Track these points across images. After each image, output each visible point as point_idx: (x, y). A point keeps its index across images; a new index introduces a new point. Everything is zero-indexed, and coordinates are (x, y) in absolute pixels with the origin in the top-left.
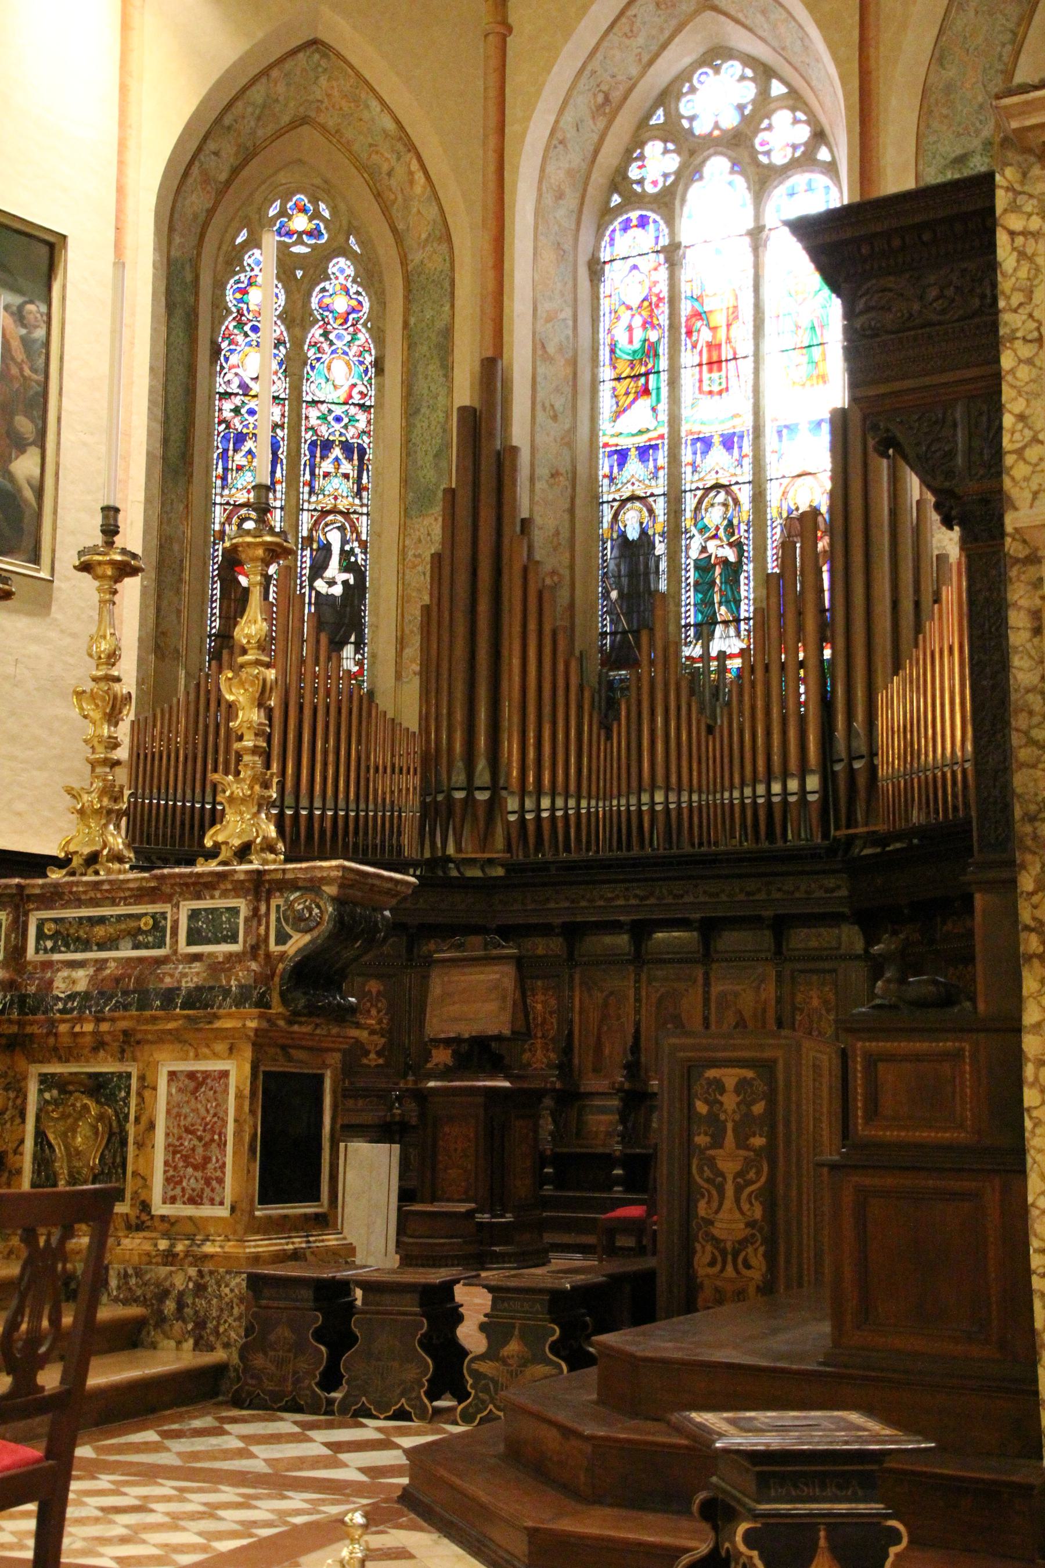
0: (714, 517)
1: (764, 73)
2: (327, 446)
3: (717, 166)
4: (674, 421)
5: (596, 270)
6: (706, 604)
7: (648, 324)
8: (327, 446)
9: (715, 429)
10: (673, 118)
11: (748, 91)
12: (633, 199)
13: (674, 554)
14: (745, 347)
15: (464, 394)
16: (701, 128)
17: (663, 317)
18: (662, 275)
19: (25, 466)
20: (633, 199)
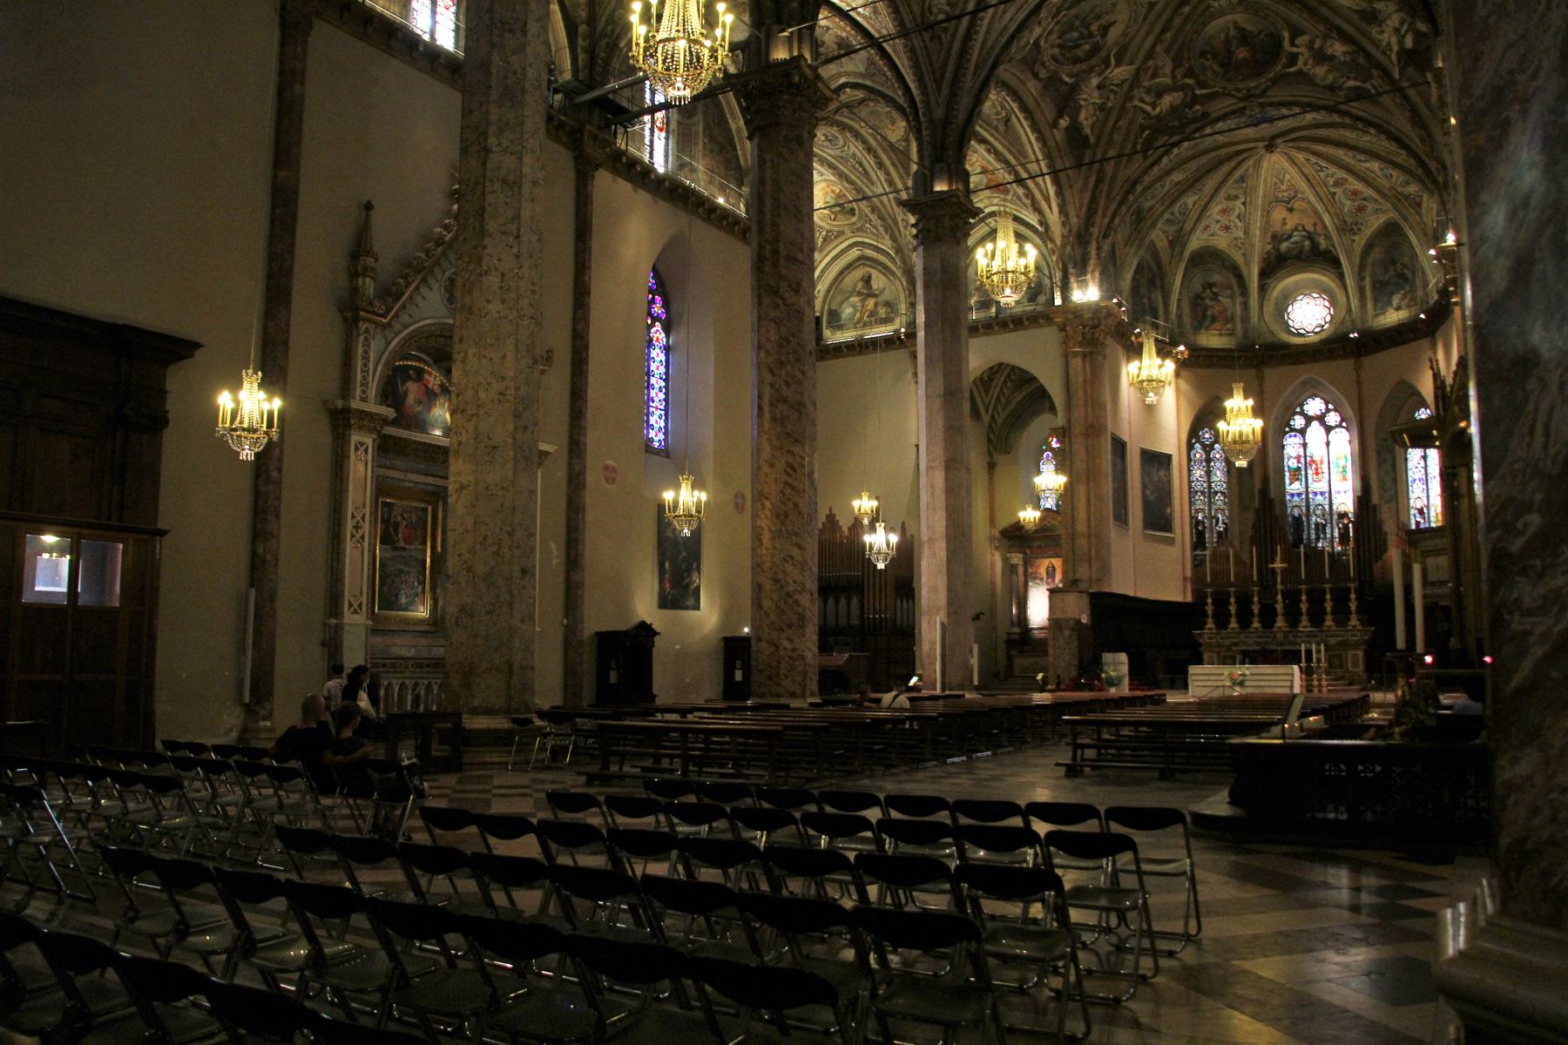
0: (1318, 512)
1: (1327, 403)
2: (1216, 493)
3: (1315, 424)
4: (1307, 487)
5: (1283, 447)
6: (1317, 534)
7: (1299, 462)
8: (1216, 493)
9: (1318, 490)
10: (1303, 410)
11: (1323, 407)
12: (1293, 430)
13: (1308, 520)
14: (1326, 470)
15: (1258, 486)
16: (1311, 413)
17: (1302, 460)
18: (1302, 450)
19: (1168, 511)
20: (1293, 430)
